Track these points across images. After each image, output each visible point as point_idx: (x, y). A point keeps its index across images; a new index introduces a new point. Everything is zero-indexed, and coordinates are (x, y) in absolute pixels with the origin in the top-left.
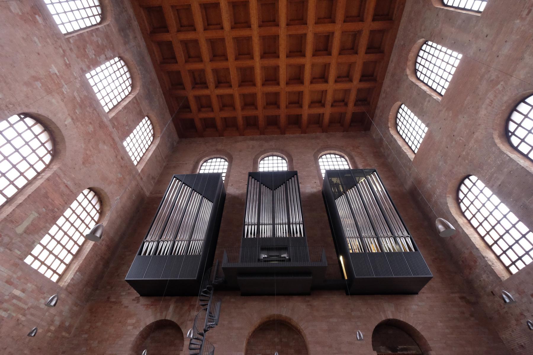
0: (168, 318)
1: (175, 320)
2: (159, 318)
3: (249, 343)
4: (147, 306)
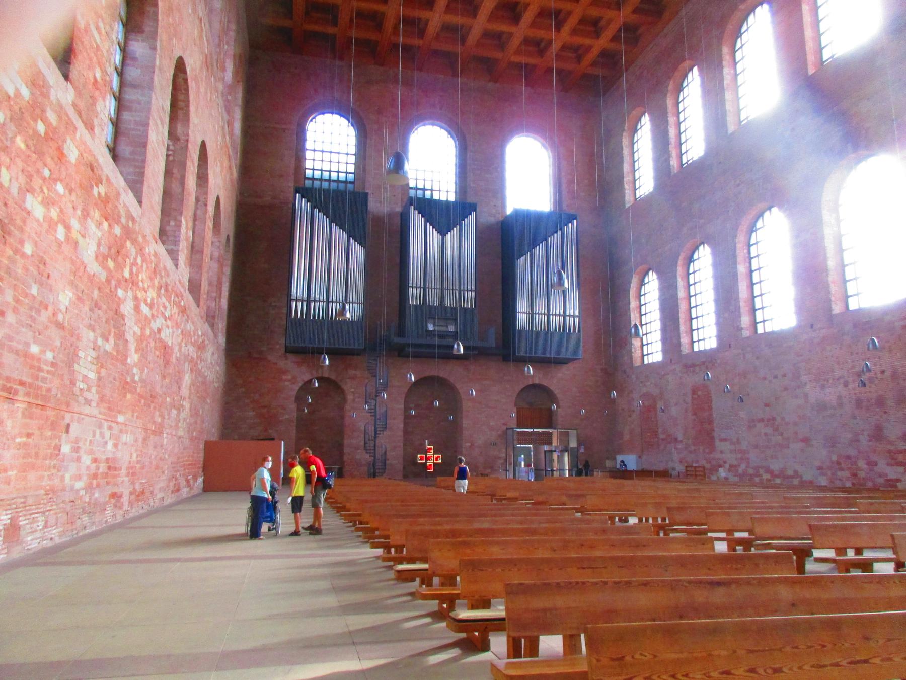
4: (299, 364)
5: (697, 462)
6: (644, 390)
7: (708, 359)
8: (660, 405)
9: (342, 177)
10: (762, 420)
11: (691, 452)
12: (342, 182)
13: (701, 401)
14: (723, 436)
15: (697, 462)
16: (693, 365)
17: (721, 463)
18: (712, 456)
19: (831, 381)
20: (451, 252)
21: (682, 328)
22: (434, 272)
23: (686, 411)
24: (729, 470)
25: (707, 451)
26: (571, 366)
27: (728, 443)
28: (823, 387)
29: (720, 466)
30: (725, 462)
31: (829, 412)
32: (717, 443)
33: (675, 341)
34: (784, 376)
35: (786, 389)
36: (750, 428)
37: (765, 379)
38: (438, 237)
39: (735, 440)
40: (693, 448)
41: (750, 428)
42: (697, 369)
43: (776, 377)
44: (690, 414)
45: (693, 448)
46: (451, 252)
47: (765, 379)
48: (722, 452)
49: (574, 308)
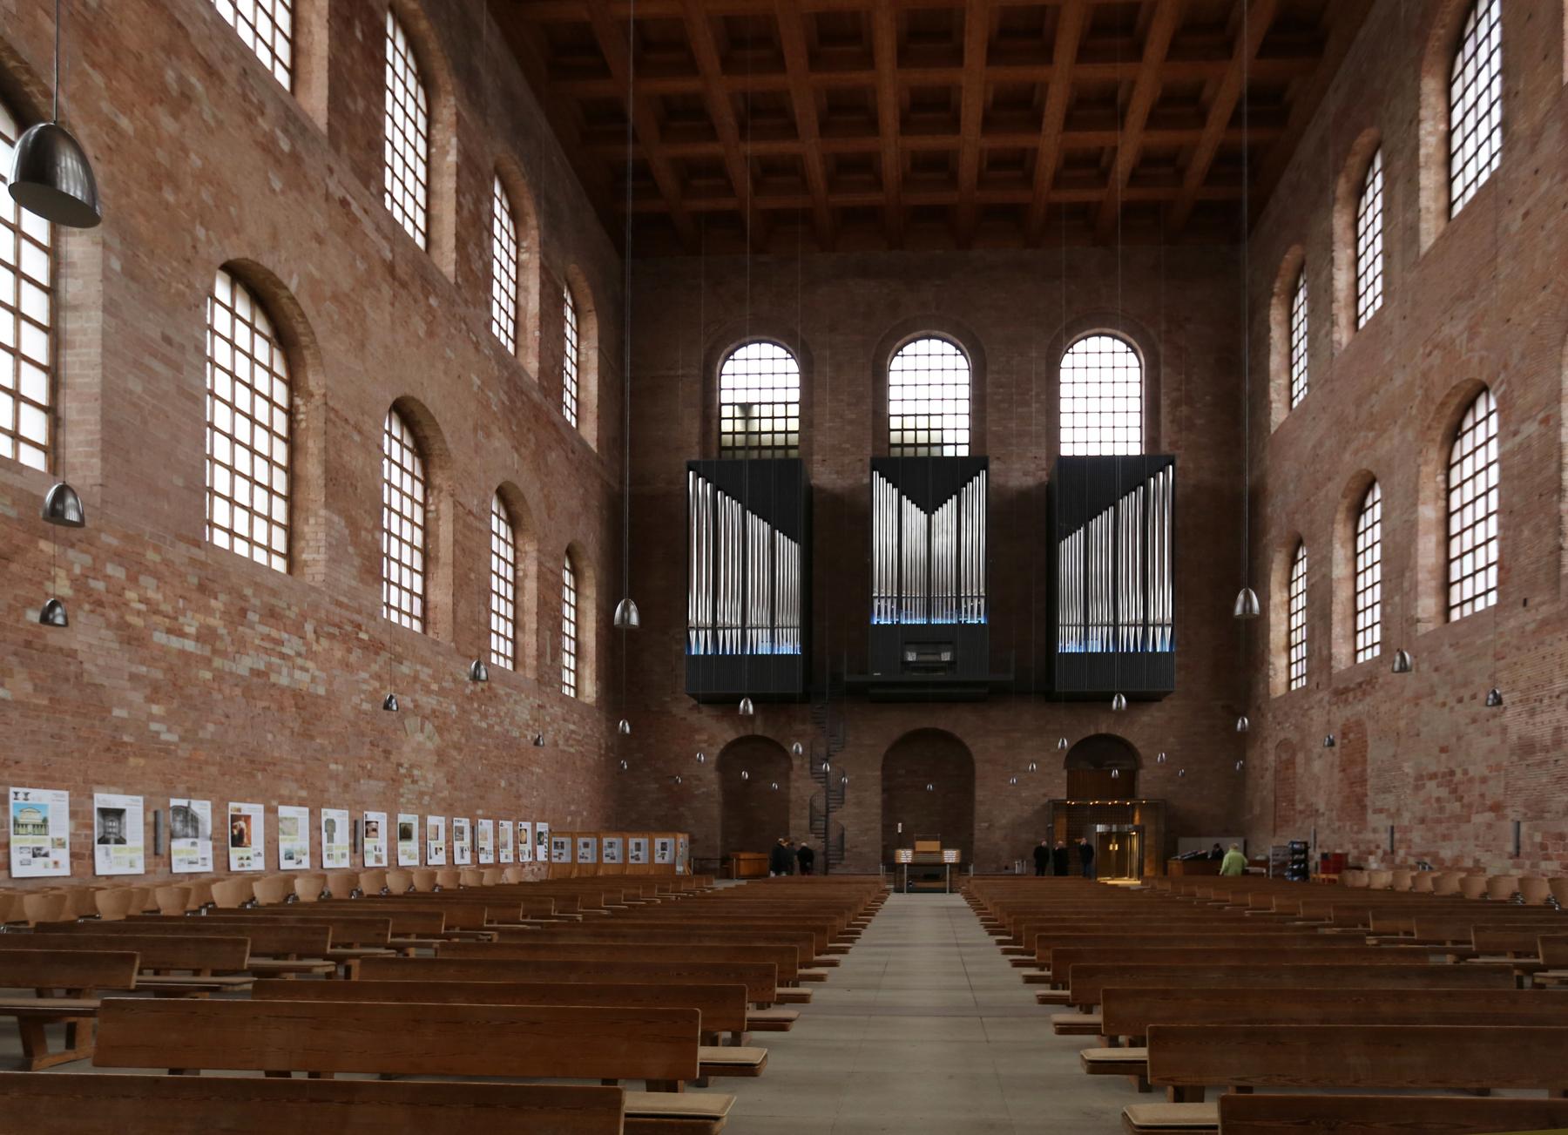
0: (759, 733)
1: (769, 735)
2: (742, 733)
3: (886, 758)
5: (1341, 846)
6: (1282, 736)
7: (1365, 681)
8: (1300, 758)
9: (780, 439)
10: (1433, 776)
11: (1334, 831)
12: (780, 447)
13: (1351, 748)
14: (1379, 804)
15: (1341, 846)
16: (1346, 690)
17: (1373, 847)
18: (1361, 836)
19: (1546, 701)
20: (944, 542)
21: (1337, 630)
22: (914, 574)
23: (1332, 766)
24: (1383, 860)
25: (1355, 828)
26: (1166, 703)
27: (1383, 816)
28: (1532, 713)
29: (1371, 853)
30: (1378, 847)
31: (1540, 756)
32: (1370, 816)
33: (1325, 652)
34: (1474, 697)
35: (1474, 721)
36: (1417, 788)
37: (1444, 704)
38: (923, 516)
39: (1393, 810)
40: (1337, 824)
41: (1417, 788)
42: (1351, 695)
43: (1460, 700)
44: (1336, 770)
45: (1337, 824)
46: (944, 542)
47: (1444, 704)
48: (1375, 830)
49: (1163, 606)
